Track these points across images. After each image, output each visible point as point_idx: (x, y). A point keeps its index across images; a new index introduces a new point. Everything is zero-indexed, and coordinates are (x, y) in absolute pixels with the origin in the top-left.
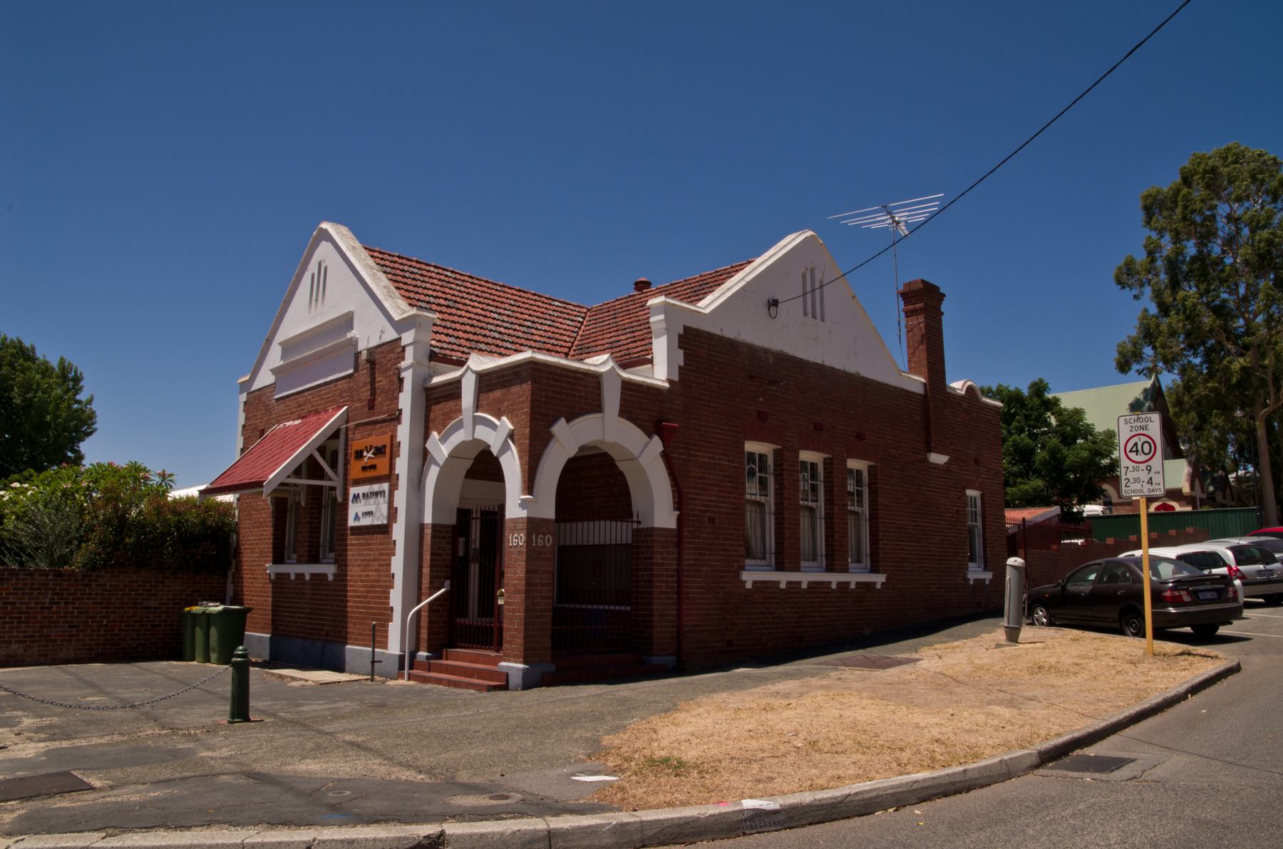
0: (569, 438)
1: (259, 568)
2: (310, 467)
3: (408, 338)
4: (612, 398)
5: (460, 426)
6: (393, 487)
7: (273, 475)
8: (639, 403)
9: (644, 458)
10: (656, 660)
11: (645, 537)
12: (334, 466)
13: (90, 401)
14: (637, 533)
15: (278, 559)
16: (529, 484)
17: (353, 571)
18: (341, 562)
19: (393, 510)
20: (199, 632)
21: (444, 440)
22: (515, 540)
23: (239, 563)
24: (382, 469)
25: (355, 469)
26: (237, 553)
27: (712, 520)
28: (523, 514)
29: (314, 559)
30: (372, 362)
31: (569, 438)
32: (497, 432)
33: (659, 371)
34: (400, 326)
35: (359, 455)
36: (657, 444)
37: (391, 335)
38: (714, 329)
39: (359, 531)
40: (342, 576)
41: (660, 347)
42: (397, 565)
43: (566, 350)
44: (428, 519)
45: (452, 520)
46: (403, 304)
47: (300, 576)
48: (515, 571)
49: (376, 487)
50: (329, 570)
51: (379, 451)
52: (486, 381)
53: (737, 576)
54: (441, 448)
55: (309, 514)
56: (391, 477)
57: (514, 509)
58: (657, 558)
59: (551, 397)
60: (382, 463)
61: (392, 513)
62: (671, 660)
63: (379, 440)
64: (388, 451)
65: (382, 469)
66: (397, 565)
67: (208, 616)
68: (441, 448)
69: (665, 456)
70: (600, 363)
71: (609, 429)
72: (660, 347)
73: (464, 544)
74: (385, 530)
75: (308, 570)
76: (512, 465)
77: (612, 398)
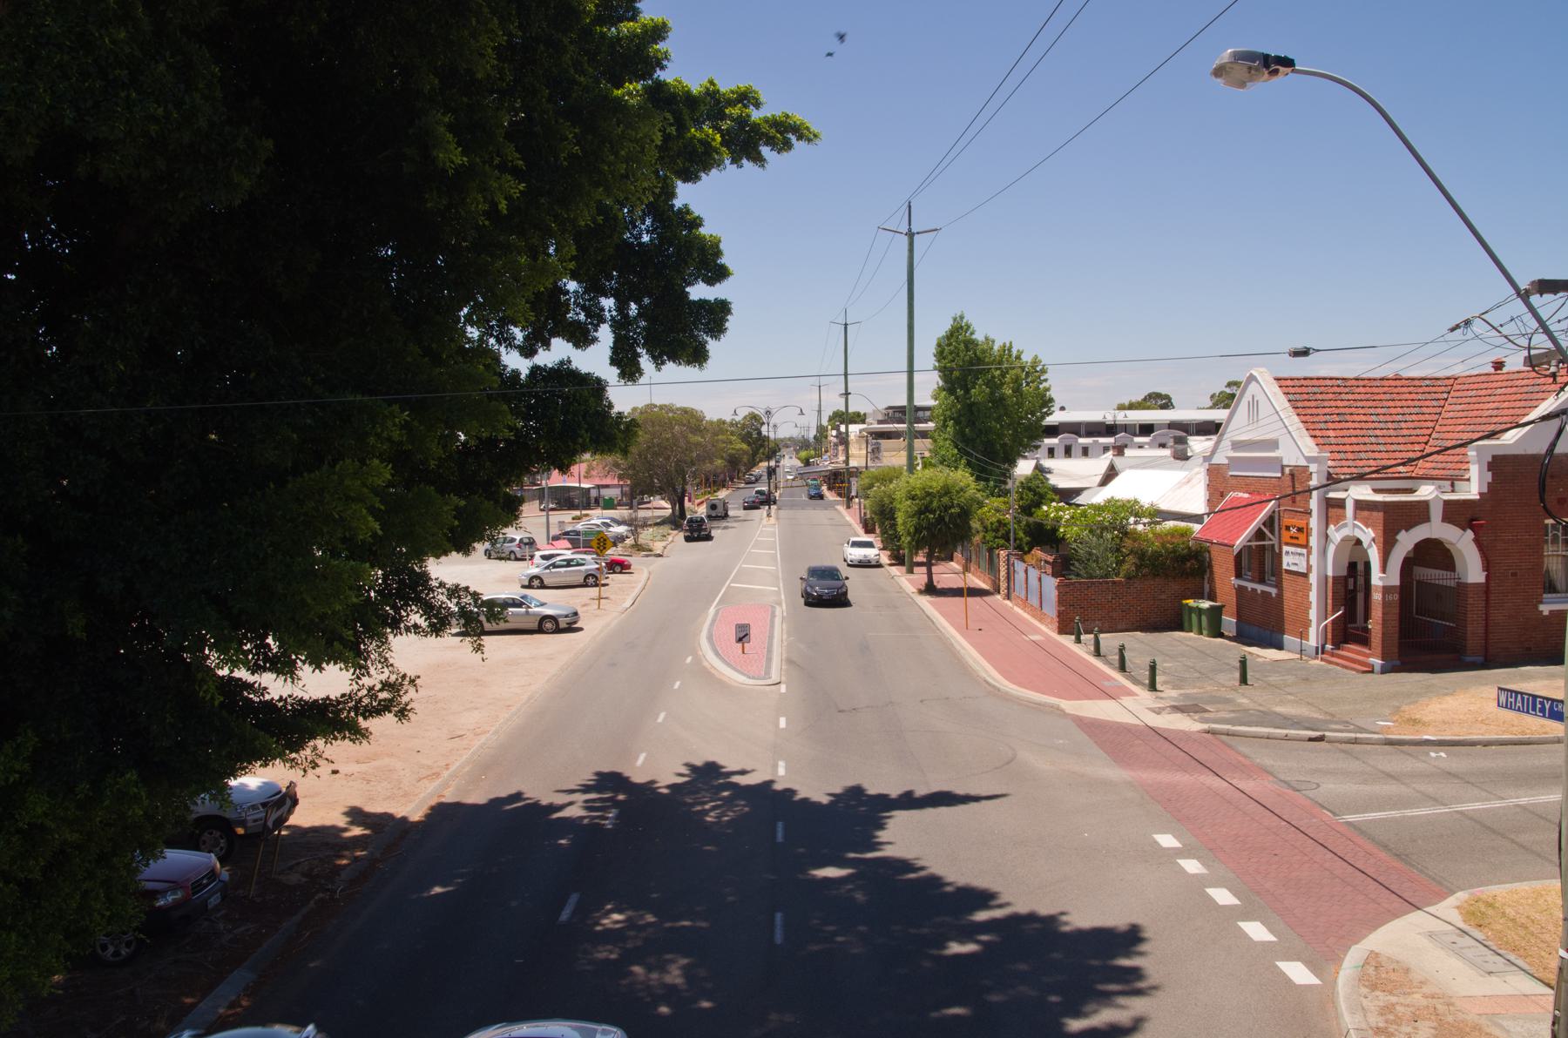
0: (1407, 541)
1: (1226, 581)
2: (1259, 534)
3: (1313, 468)
4: (1436, 513)
5: (1345, 525)
6: (1309, 553)
7: (1239, 542)
8: (1457, 513)
9: (1463, 544)
10: (1468, 659)
11: (1462, 588)
12: (1272, 532)
13: (1048, 389)
14: (1459, 584)
15: (1239, 575)
16: (1384, 569)
17: (1287, 595)
18: (1279, 585)
19: (1311, 563)
20: (1194, 617)
21: (1337, 530)
22: (1377, 597)
23: (1212, 572)
24: (1302, 541)
25: (1285, 535)
26: (1210, 566)
27: (1514, 574)
28: (1381, 584)
29: (1262, 581)
30: (1292, 475)
31: (1407, 541)
32: (1367, 535)
33: (1472, 488)
34: (1309, 459)
35: (1288, 528)
36: (1470, 534)
37: (1303, 463)
38: (1520, 451)
39: (1288, 572)
40: (1280, 595)
41: (1474, 472)
42: (1313, 596)
43: (1425, 439)
44: (1330, 573)
45: (1345, 573)
46: (1310, 442)
47: (1254, 590)
48: (1377, 613)
49: (1299, 550)
50: (1274, 591)
51: (1300, 530)
52: (1361, 506)
53: (1536, 607)
54: (1336, 535)
55: (1259, 560)
56: (1306, 546)
57: (1377, 578)
58: (1470, 601)
59: (1396, 518)
60: (1302, 537)
61: (1309, 568)
62: (1480, 659)
63: (1301, 524)
64: (1304, 530)
65: (1302, 541)
66: (1313, 596)
67: (1200, 611)
68: (1336, 535)
69: (1477, 541)
70: (1426, 492)
71: (1437, 529)
72: (1474, 472)
73: (1350, 585)
74: (1305, 575)
75: (1260, 588)
76: (1374, 555)
77: (1436, 513)
